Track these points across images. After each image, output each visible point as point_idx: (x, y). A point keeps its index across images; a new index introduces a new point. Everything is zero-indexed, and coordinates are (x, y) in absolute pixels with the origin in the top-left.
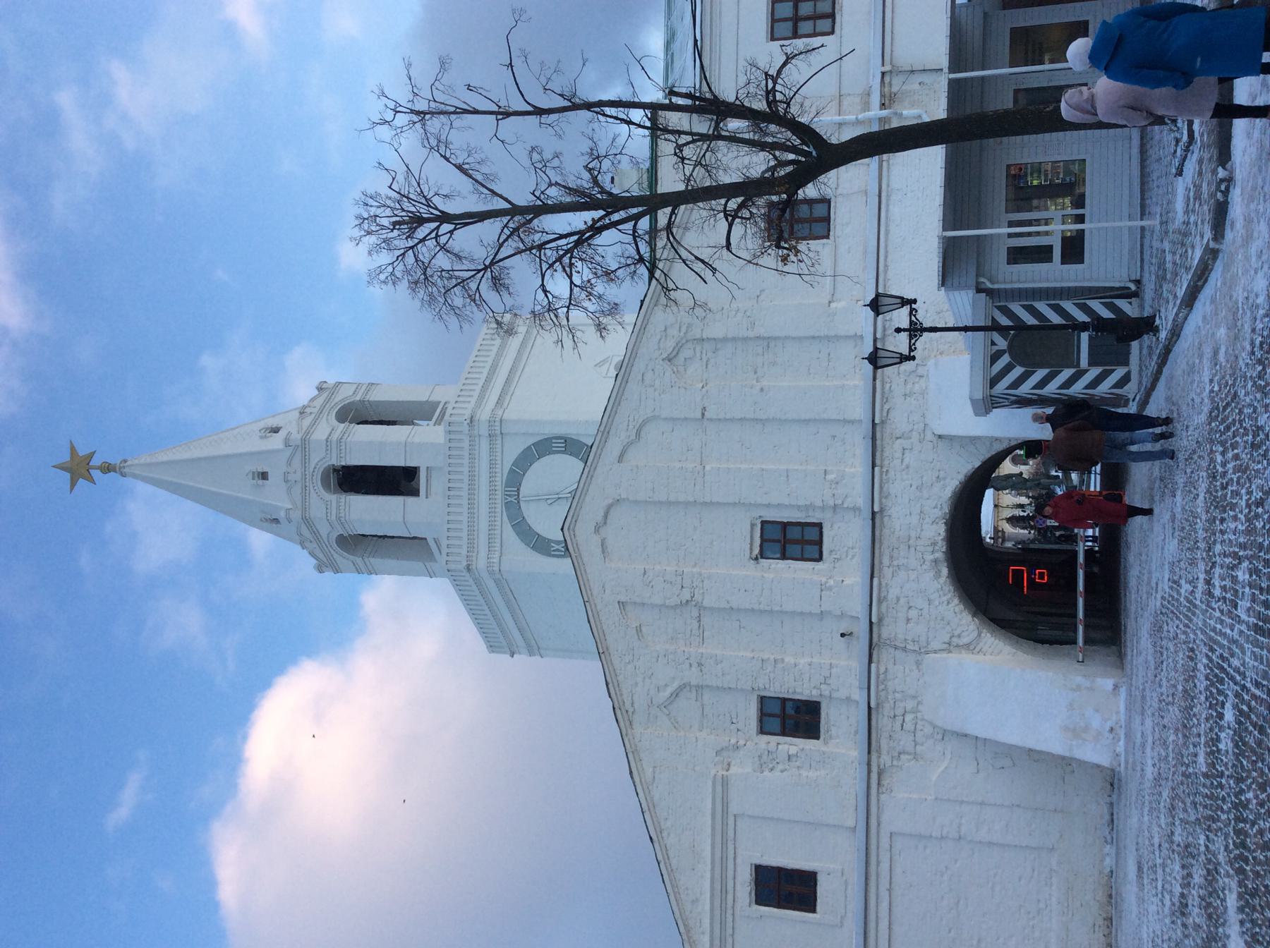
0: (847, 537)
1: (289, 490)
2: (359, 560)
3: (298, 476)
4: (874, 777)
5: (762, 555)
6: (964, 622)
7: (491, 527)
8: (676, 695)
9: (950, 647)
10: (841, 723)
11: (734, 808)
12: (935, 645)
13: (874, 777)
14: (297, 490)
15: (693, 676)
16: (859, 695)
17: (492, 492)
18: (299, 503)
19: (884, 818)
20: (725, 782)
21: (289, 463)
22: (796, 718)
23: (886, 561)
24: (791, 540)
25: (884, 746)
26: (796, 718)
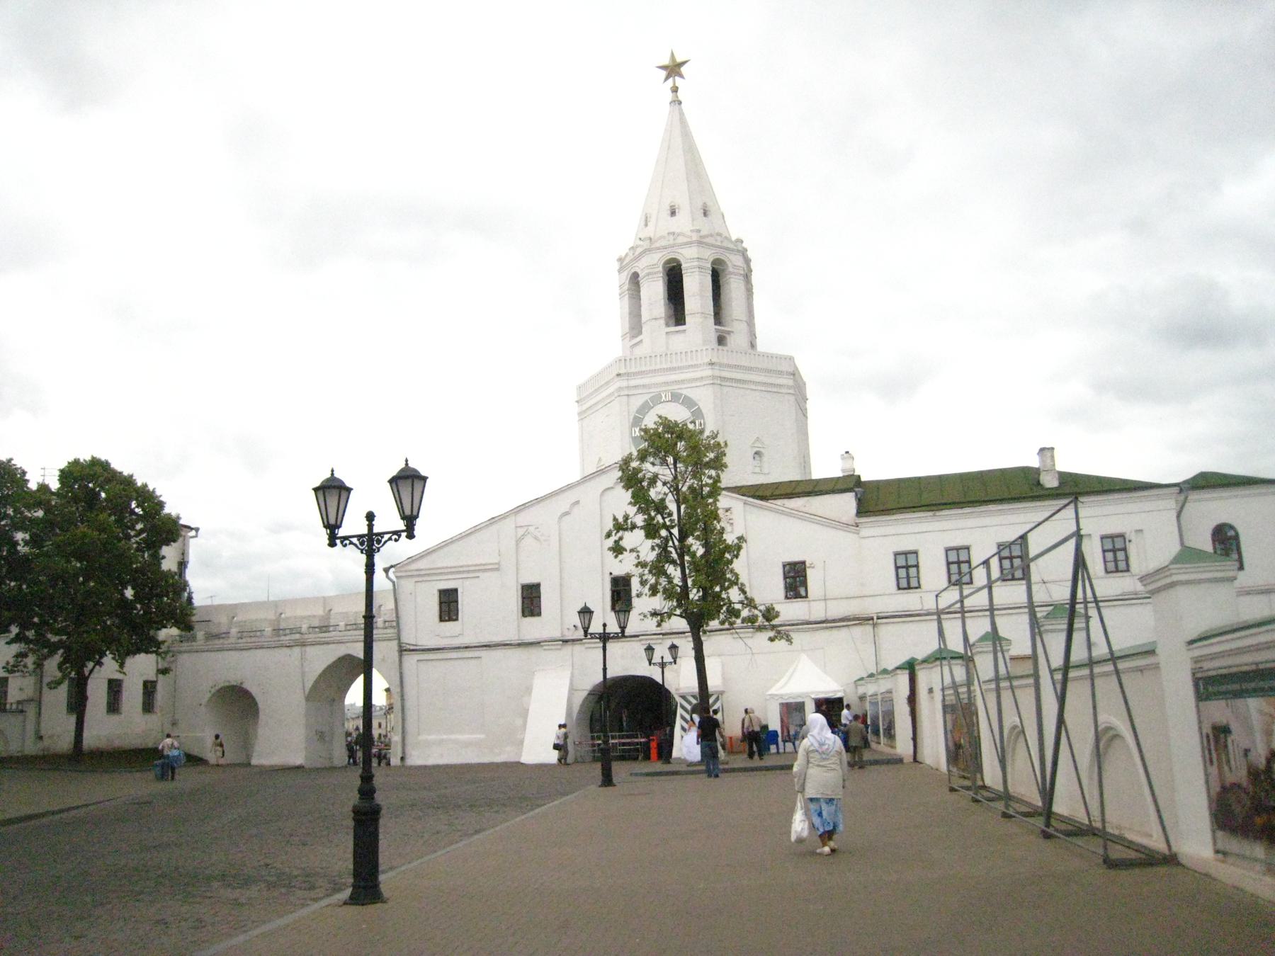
3: (672, 242)
7: (644, 386)
14: (664, 243)
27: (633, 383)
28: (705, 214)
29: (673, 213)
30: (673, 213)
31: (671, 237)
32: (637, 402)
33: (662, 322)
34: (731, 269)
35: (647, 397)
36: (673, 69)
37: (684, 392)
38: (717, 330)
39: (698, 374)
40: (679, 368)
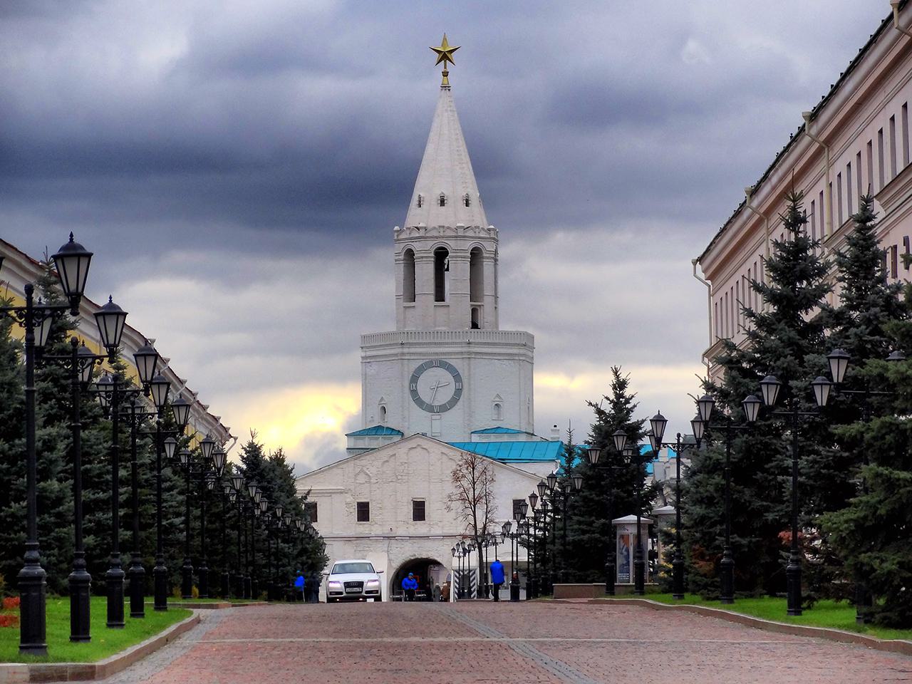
0: (420, 528)
1: (435, 228)
2: (402, 257)
4: (348, 539)
5: (414, 502)
6: (397, 564)
7: (420, 354)
8: (367, 474)
9: (390, 560)
10: (363, 529)
11: (333, 495)
12: (390, 555)
13: (348, 539)
14: (436, 234)
15: (373, 480)
16: (373, 534)
17: (437, 354)
18: (427, 235)
19: (336, 542)
20: (341, 493)
21: (448, 228)
22: (363, 512)
23: (415, 541)
24: (419, 511)
25: (358, 541)
26: (363, 512)
27: (412, 350)
28: (467, 205)
29: (442, 202)
30: (442, 202)
31: (442, 230)
32: (415, 365)
33: (433, 297)
34: (485, 255)
35: (421, 362)
36: (445, 57)
37: (453, 362)
38: (472, 305)
39: (459, 350)
40: (447, 343)
